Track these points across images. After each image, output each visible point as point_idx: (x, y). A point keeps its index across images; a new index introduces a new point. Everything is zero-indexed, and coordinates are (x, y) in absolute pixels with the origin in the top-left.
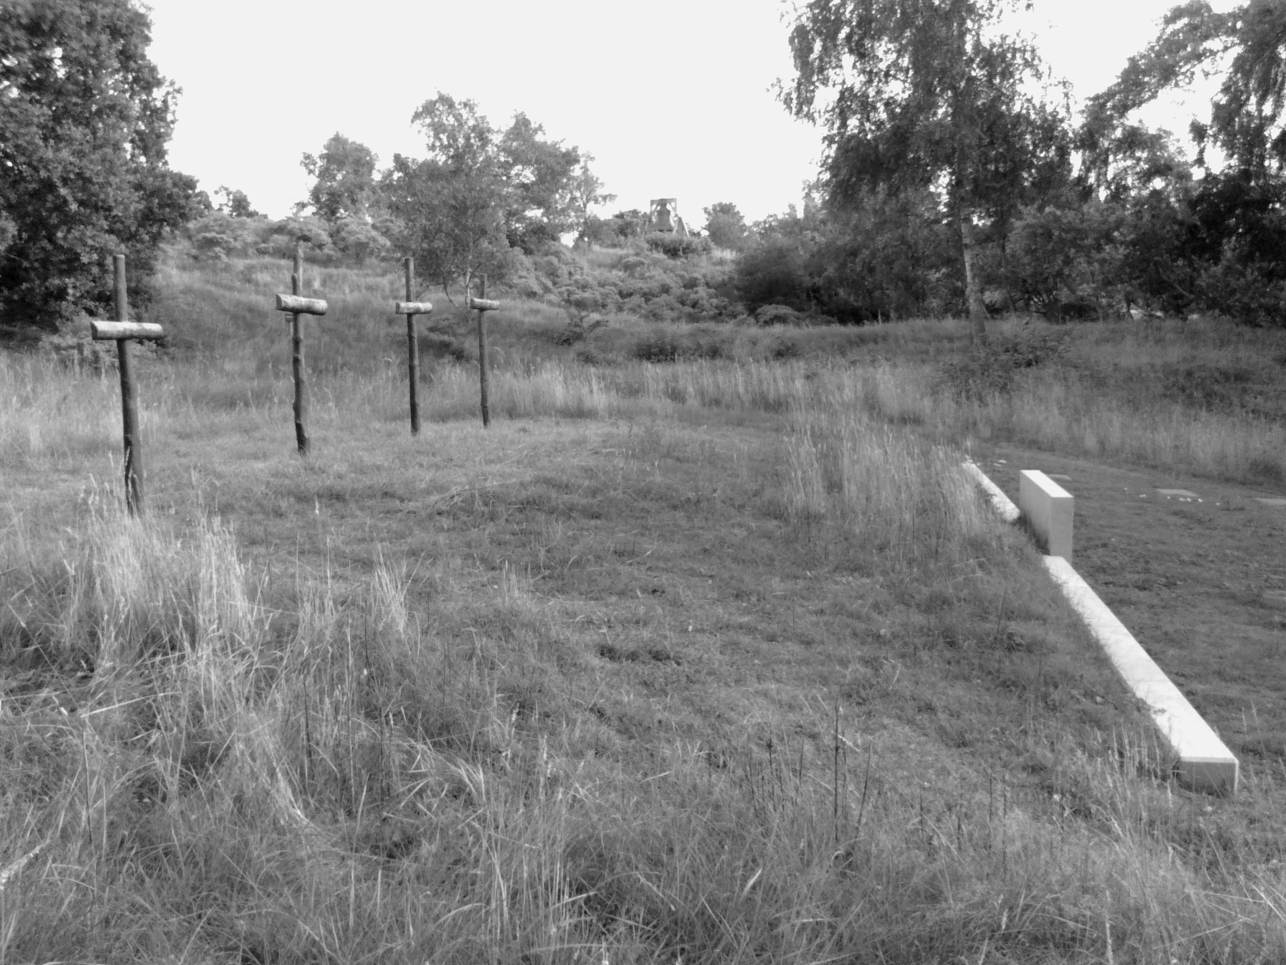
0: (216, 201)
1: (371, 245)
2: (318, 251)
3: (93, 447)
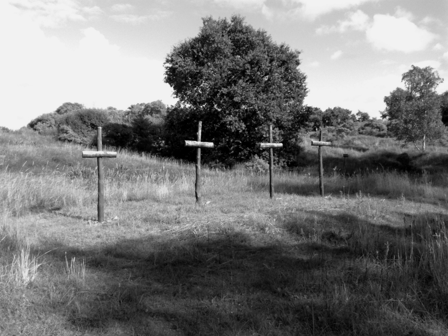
0: (357, 117)
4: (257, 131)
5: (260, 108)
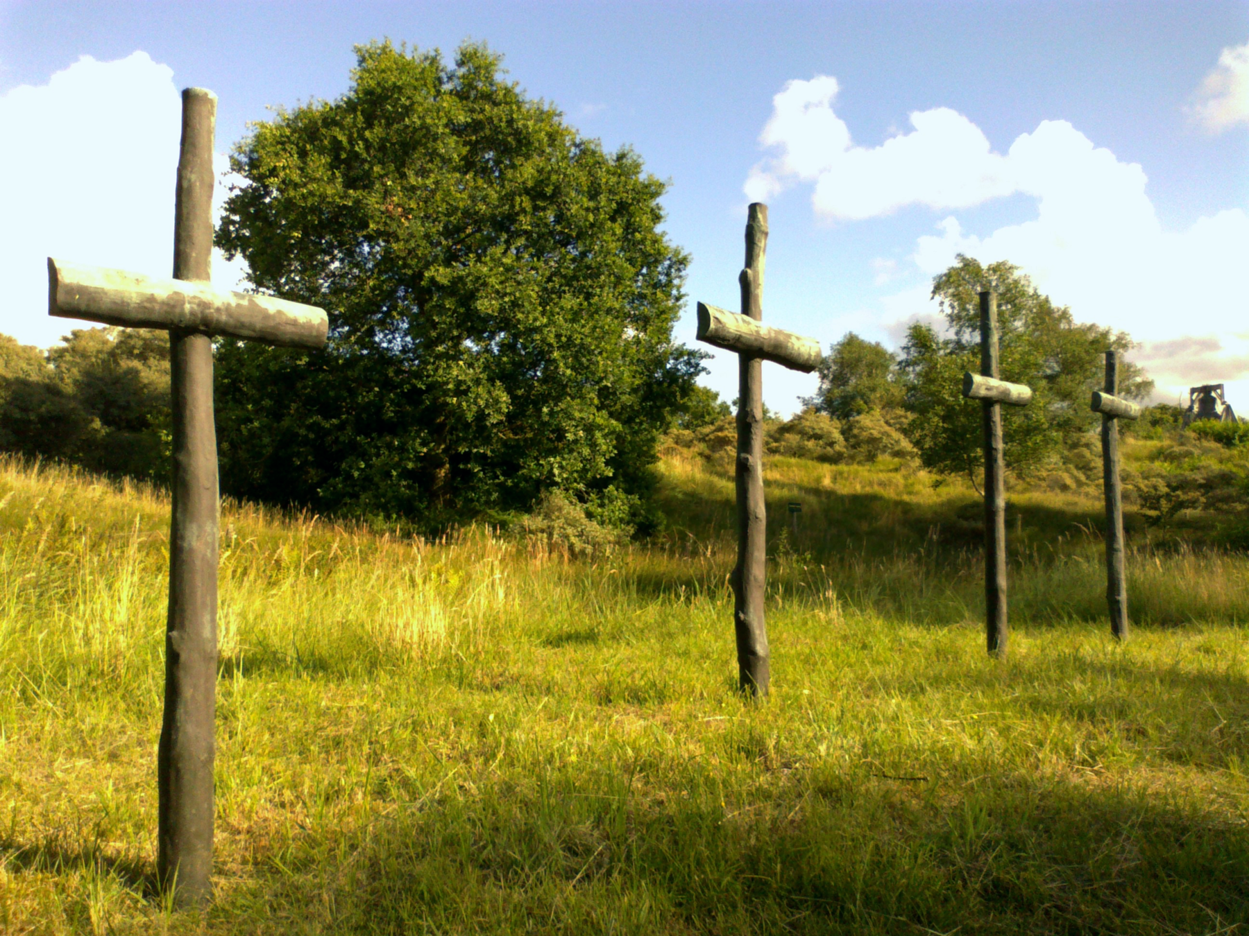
2: (829, 449)
4: (546, 419)
5: (564, 339)
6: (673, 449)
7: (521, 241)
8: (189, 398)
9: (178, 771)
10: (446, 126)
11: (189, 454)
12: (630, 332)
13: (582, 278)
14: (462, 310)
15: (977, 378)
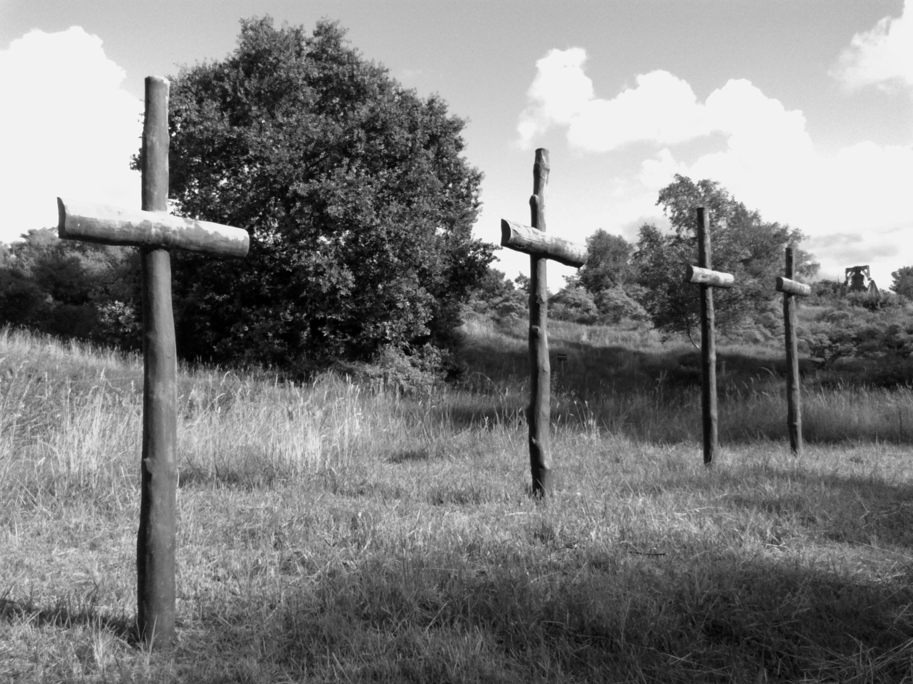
0: (517, 286)
1: (626, 307)
2: (586, 314)
3: (192, 477)
5: (392, 234)
6: (473, 315)
7: (359, 162)
8: (154, 292)
9: (151, 556)
10: (304, 79)
11: (156, 333)
12: (441, 231)
13: (403, 190)
14: (317, 214)
15: (696, 269)
